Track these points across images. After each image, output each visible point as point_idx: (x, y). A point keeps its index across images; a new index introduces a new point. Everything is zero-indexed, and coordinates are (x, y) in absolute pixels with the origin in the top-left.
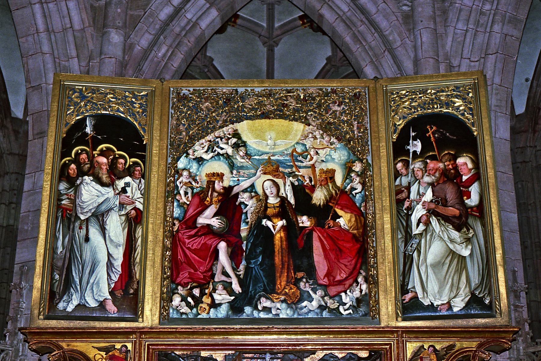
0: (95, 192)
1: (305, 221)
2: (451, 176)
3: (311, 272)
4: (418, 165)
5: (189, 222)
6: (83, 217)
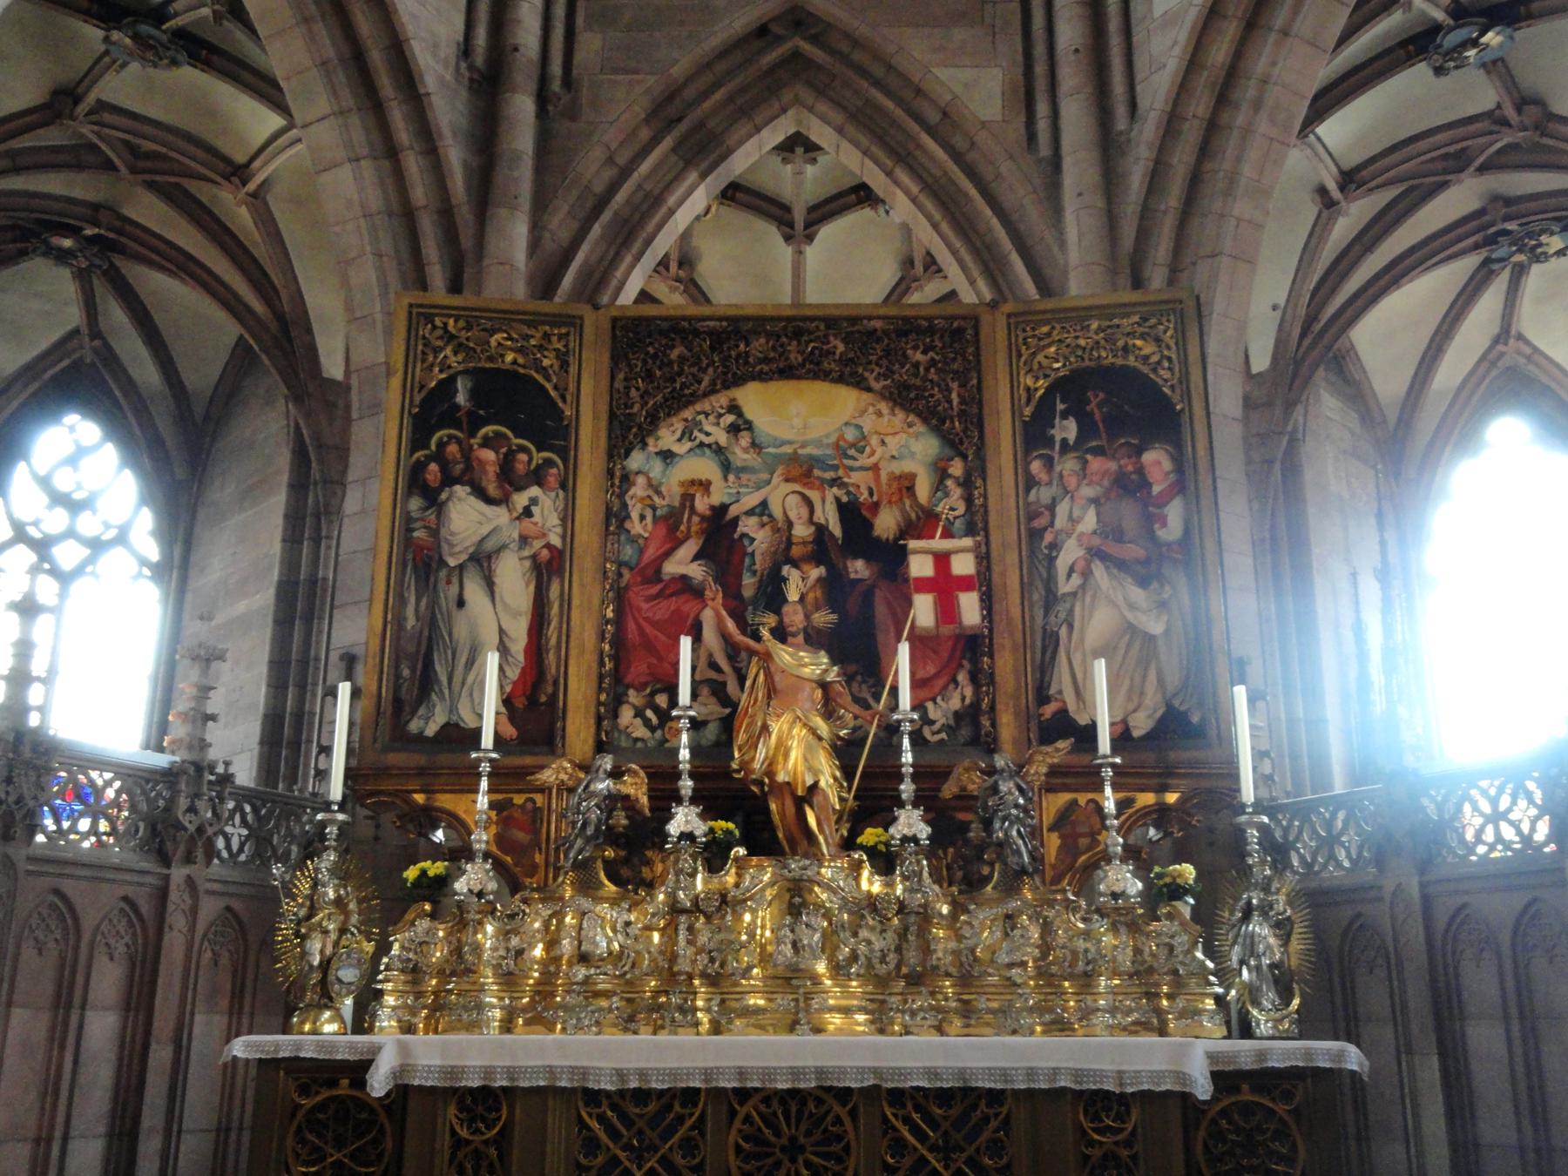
0: (475, 517)
1: (858, 568)
4: (1068, 465)
6: (452, 562)
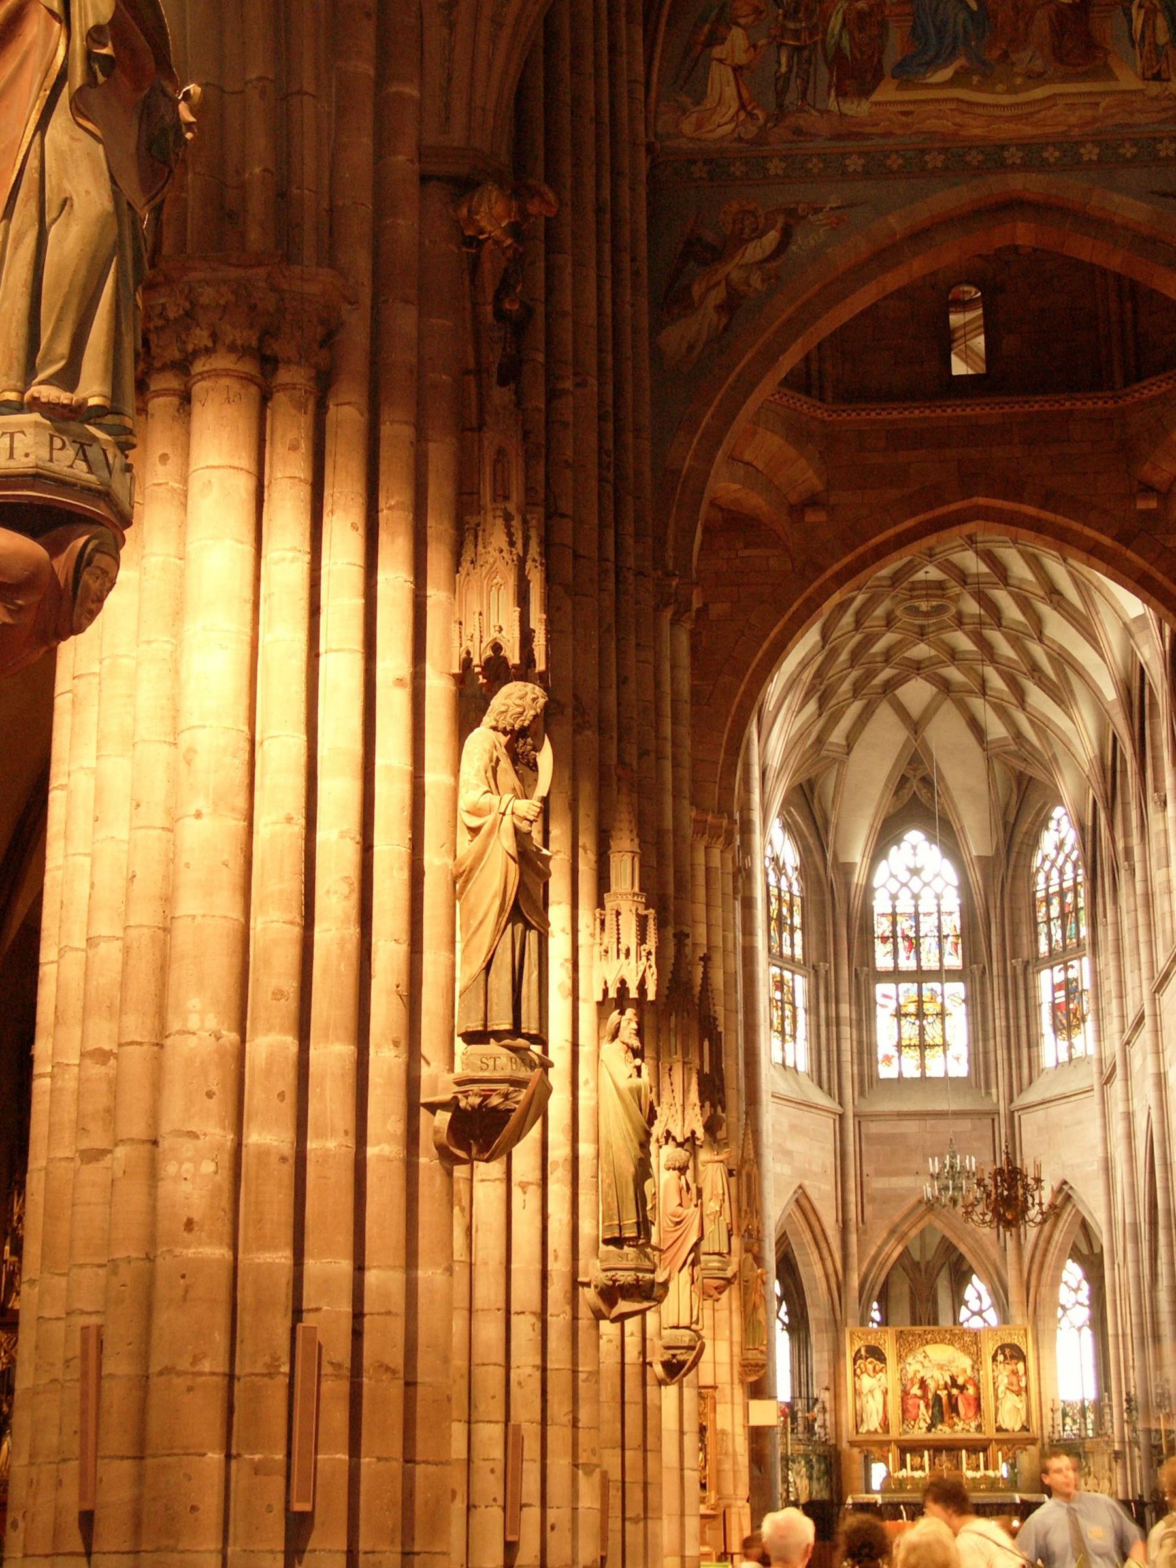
1: (955, 1391)
2: (1015, 1373)
3: (958, 1414)
4: (1001, 1367)
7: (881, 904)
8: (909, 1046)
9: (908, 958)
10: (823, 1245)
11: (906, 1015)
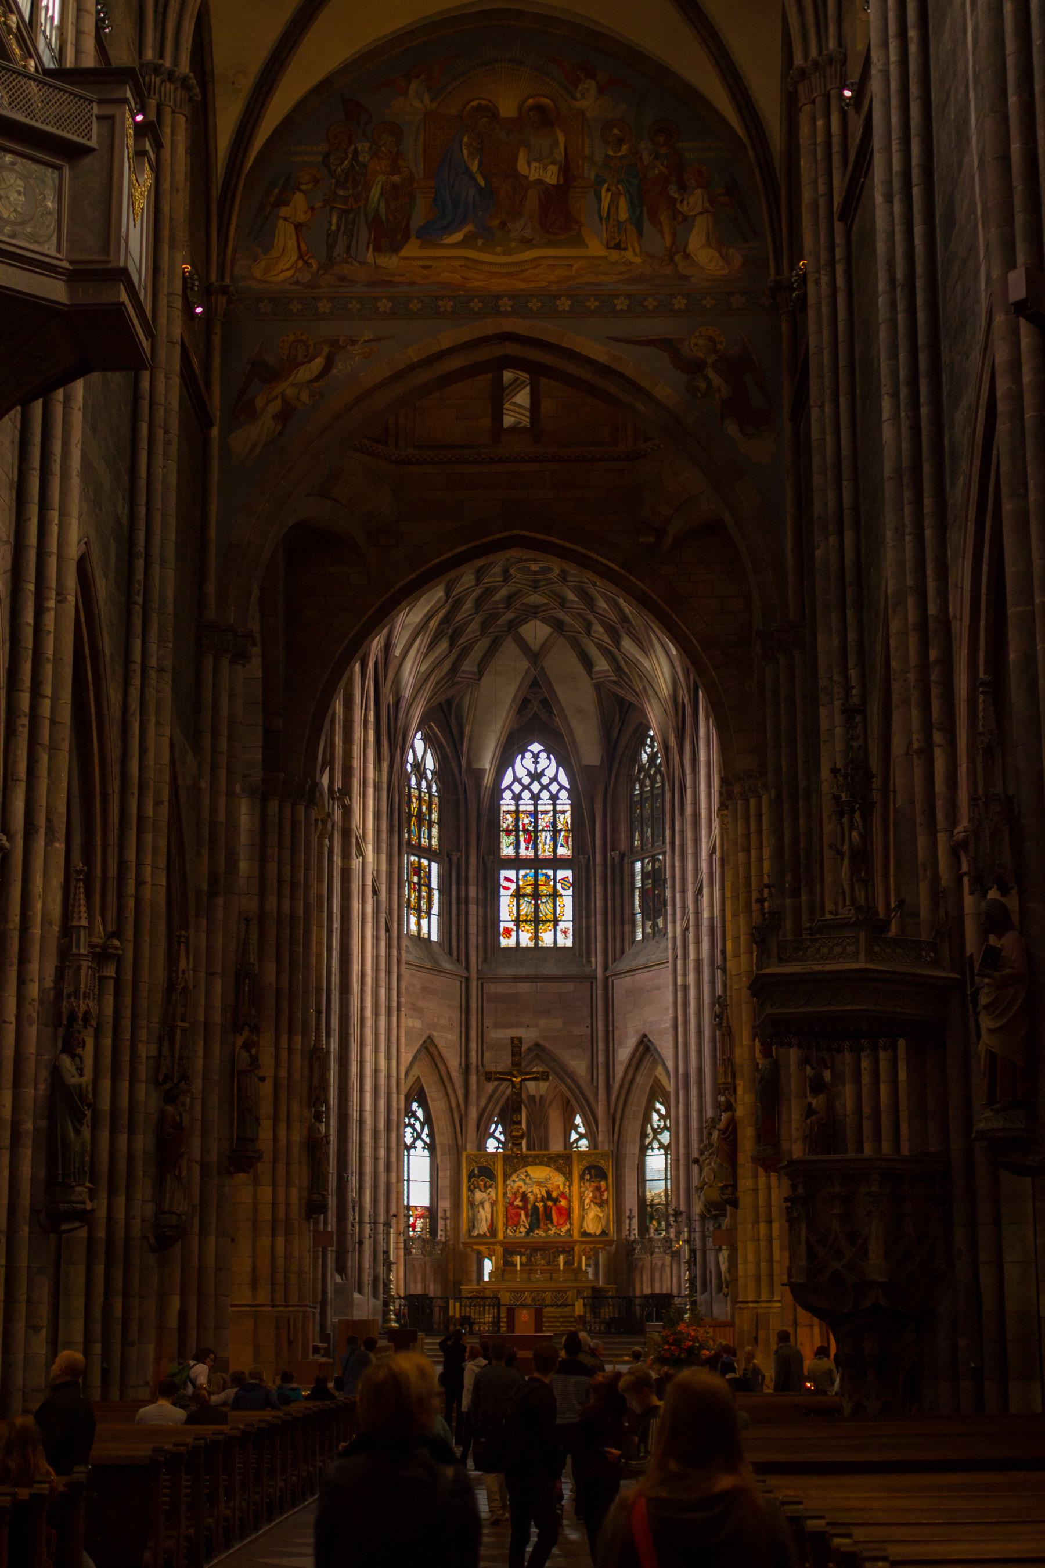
1: (550, 1203)
2: (598, 1188)
3: (552, 1222)
4: (587, 1184)
5: (512, 1204)
7: (507, 801)
8: (526, 921)
9: (527, 848)
10: (448, 1084)
11: (525, 895)
